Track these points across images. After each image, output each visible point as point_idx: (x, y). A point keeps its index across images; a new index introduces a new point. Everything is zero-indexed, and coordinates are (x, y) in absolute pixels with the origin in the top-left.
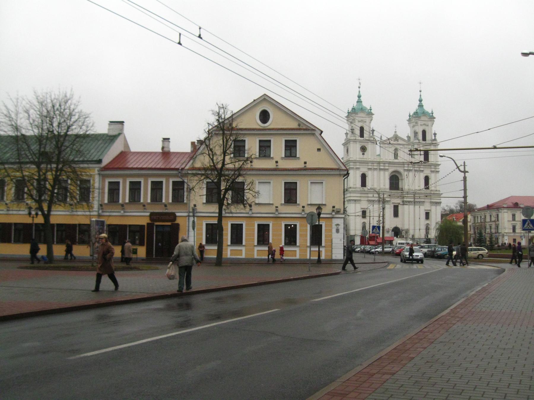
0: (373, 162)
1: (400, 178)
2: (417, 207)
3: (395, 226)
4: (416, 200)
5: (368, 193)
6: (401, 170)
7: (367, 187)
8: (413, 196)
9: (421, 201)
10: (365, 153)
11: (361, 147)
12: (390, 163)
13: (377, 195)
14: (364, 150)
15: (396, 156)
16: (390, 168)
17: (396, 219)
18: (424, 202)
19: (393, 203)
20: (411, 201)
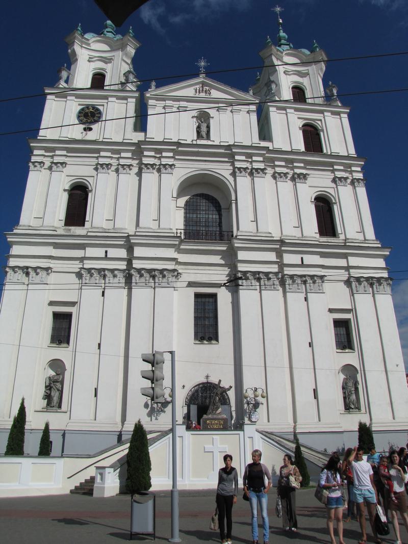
0: (116, 148)
1: (223, 205)
2: (295, 298)
3: (203, 380)
4: (288, 271)
5: (82, 247)
6: (223, 170)
7: (87, 224)
8: (272, 256)
9: (312, 277)
10: (95, 127)
11: (83, 109)
12: (178, 149)
13: (123, 253)
14: (93, 115)
15: (203, 129)
16: (178, 164)
17: (207, 348)
18: (322, 277)
19: (191, 284)
20: (267, 274)
